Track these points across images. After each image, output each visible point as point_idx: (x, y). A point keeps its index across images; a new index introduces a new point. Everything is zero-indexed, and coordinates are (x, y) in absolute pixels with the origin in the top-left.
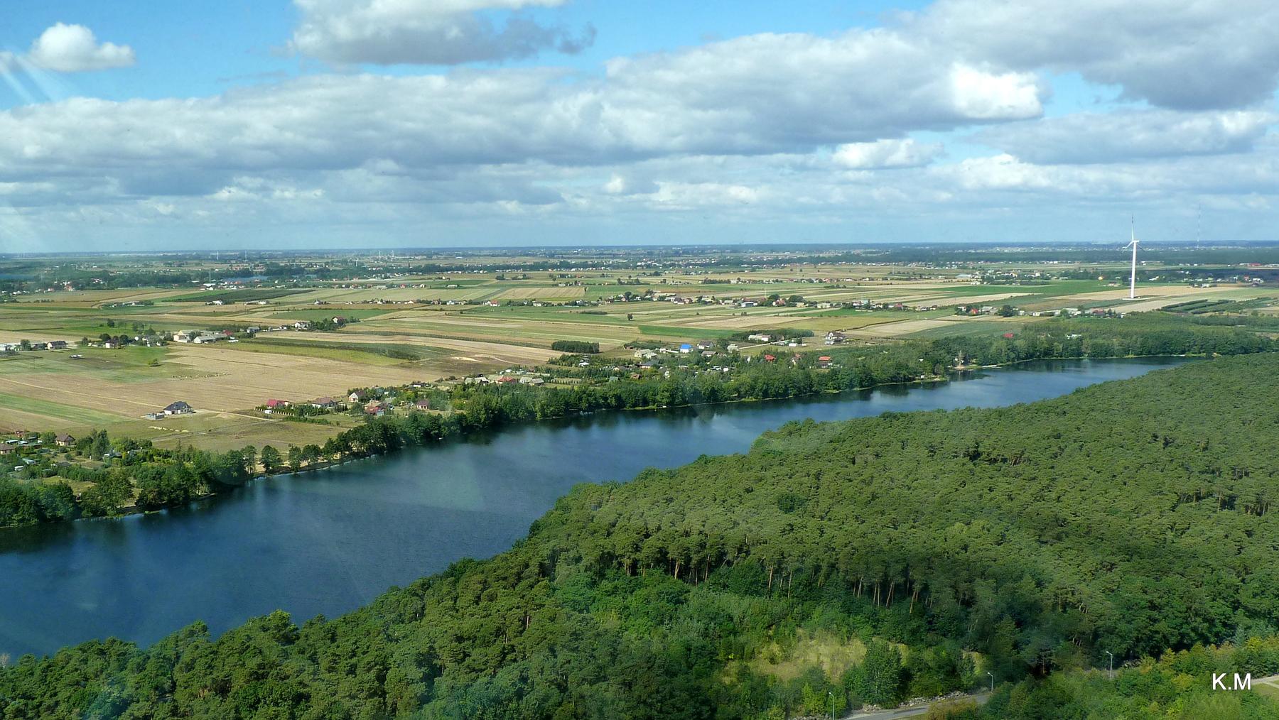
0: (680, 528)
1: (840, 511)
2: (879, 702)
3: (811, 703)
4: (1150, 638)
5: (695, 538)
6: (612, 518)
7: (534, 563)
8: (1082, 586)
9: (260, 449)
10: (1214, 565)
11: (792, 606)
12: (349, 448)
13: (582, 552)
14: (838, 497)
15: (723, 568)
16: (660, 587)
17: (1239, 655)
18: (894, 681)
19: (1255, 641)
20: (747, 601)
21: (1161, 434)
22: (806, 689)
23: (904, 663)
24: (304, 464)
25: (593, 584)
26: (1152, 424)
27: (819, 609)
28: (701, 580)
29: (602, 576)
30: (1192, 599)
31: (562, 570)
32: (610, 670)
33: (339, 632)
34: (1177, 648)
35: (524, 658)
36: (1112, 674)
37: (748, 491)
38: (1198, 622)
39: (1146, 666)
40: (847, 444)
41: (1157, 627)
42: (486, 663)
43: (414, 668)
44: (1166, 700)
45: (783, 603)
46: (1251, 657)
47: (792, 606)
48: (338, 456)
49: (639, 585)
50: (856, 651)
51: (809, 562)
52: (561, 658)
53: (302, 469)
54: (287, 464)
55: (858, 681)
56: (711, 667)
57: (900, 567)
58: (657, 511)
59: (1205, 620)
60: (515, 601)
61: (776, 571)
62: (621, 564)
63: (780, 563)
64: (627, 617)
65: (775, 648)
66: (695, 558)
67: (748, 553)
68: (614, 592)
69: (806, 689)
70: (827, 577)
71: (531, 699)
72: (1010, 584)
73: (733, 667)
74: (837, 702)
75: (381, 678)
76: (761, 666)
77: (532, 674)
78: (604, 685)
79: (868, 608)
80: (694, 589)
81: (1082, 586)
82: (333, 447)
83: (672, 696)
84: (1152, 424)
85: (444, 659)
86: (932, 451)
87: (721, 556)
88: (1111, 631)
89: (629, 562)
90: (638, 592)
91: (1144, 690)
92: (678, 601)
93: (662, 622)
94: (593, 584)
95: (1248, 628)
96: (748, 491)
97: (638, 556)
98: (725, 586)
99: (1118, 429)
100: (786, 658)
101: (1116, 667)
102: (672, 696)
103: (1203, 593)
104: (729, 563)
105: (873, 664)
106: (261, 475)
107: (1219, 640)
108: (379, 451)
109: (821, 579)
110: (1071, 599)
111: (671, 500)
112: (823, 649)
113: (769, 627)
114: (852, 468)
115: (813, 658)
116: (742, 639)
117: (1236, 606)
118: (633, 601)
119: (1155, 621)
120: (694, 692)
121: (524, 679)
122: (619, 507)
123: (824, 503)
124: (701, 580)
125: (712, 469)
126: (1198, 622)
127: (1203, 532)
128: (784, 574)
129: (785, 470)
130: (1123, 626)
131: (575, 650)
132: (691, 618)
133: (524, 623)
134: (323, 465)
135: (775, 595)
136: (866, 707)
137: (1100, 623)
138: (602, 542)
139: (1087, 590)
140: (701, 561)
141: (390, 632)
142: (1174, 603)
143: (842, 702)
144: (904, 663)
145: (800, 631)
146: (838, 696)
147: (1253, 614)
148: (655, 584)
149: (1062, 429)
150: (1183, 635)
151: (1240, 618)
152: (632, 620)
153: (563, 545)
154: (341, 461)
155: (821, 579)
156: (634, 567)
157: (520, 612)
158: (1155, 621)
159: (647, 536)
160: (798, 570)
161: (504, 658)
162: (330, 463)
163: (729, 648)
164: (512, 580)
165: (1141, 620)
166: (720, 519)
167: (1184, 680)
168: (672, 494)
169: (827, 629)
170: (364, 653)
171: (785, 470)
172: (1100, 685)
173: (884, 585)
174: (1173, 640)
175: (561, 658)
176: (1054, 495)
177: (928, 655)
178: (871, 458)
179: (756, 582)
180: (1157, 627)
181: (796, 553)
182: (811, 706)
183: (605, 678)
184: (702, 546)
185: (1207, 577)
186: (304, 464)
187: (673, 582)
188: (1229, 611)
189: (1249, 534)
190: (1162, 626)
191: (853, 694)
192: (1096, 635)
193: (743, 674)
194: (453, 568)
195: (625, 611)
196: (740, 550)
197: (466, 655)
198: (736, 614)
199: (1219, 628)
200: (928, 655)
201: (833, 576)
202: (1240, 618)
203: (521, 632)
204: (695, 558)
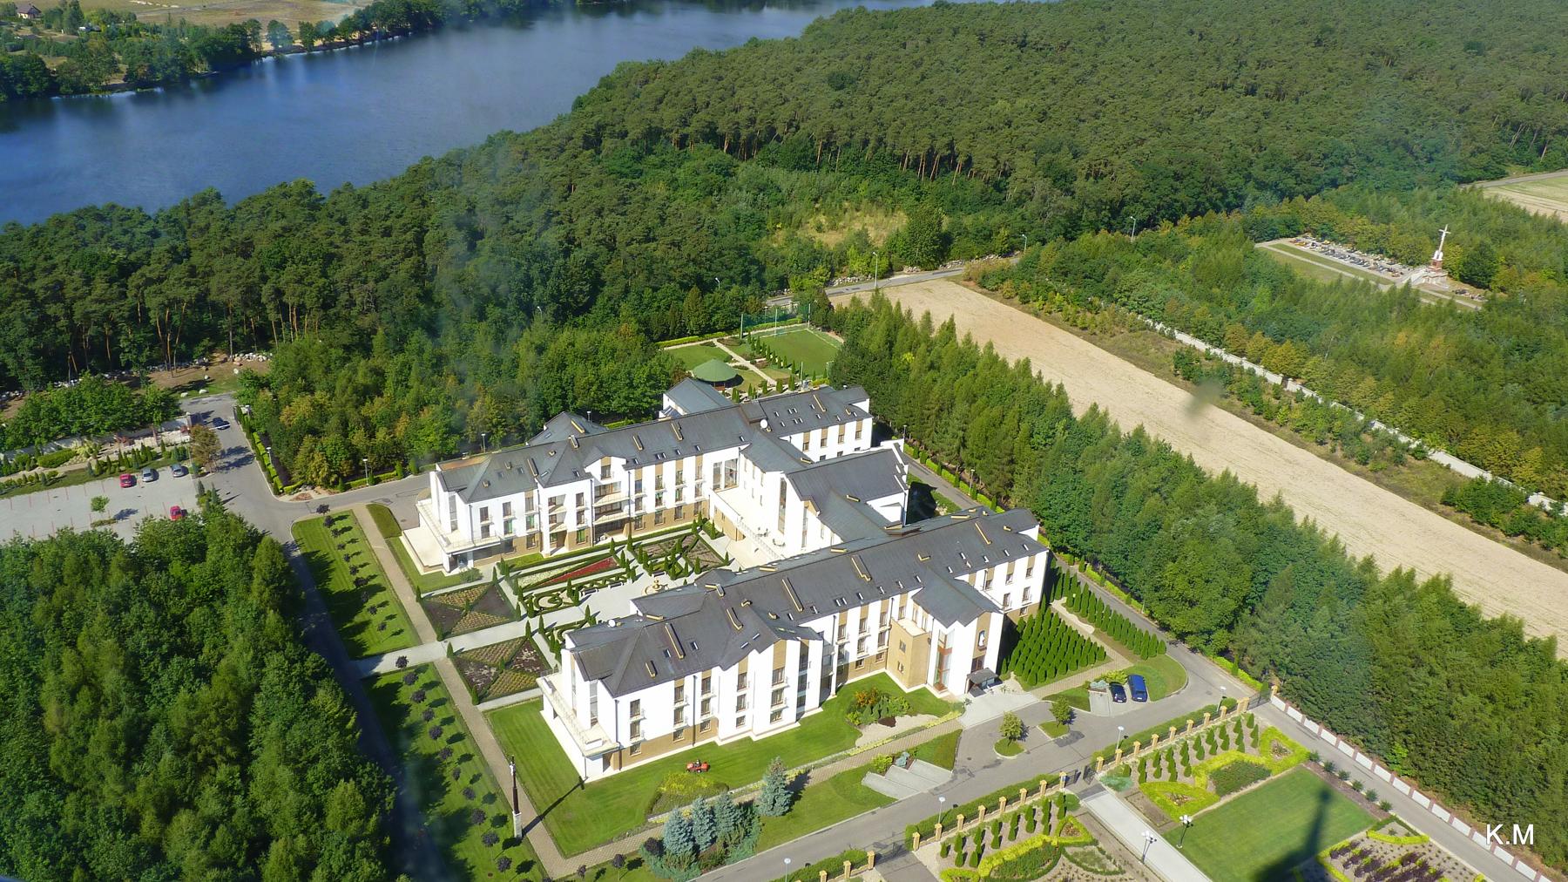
0: (730, 103)
1: (889, 90)
2: (919, 264)
3: (856, 265)
4: (1170, 206)
5: (745, 113)
6: (660, 93)
7: (578, 134)
8: (1113, 158)
9: (265, 26)
10: (1234, 140)
11: (839, 179)
12: (369, 28)
13: (628, 128)
14: (888, 78)
15: (773, 144)
16: (709, 160)
17: (1245, 221)
18: (935, 243)
19: (1260, 209)
20: (795, 175)
21: (1197, 29)
22: (851, 251)
23: (944, 228)
24: (318, 43)
25: (639, 159)
26: (1191, 20)
27: (866, 183)
28: (750, 156)
29: (650, 151)
30: (1211, 170)
31: (607, 143)
32: (659, 231)
33: (371, 199)
34: (1192, 215)
35: (571, 221)
36: (1133, 239)
37: (798, 70)
38: (1214, 194)
39: (1165, 229)
40: (899, 31)
41: (1178, 196)
42: (530, 225)
43: (454, 229)
44: (1179, 258)
45: (831, 178)
46: (1256, 223)
47: (839, 179)
48: (356, 35)
49: (688, 158)
50: (900, 222)
51: (858, 136)
52: (607, 220)
53: (317, 49)
54: (298, 43)
55: (900, 244)
56: (759, 235)
57: (946, 140)
58: (705, 87)
59: (1220, 190)
60: (559, 169)
61: (825, 146)
62: (668, 139)
63: (829, 136)
64: (675, 189)
65: (823, 219)
66: (744, 133)
67: (798, 128)
68: (663, 164)
69: (851, 251)
70: (875, 150)
71: (579, 255)
72: (1049, 156)
73: (781, 235)
74: (880, 264)
75: (419, 240)
76: (808, 232)
77: (579, 234)
78: (653, 245)
79: (912, 181)
80: (743, 164)
81: (1113, 158)
82: (349, 25)
83: (721, 255)
84: (1191, 20)
85: (484, 220)
86: (982, 38)
87: (772, 131)
88: (1136, 199)
89: (677, 136)
90: (687, 164)
91: (1162, 250)
92: (727, 173)
93: (711, 193)
94: (639, 159)
95: (1255, 199)
96: (798, 70)
97: (686, 130)
98: (774, 162)
99: (1159, 23)
100: (833, 227)
101: (1136, 234)
102: (721, 255)
103: (1221, 164)
104: (779, 139)
105: (913, 232)
106: (269, 54)
107: (1230, 208)
108: (403, 32)
109: (869, 152)
110: (1103, 170)
111: (720, 79)
112: (868, 219)
113: (816, 200)
114: (902, 52)
115: (857, 227)
116: (790, 208)
117: (1248, 177)
118: (681, 174)
119: (1176, 190)
120: (742, 251)
121: (571, 241)
122: (667, 84)
123: (875, 81)
124: (750, 156)
125: (761, 51)
126: (1214, 194)
127: (1226, 114)
128: (833, 149)
129: (836, 51)
130: (1147, 195)
131: (624, 214)
132: (740, 189)
133: (570, 188)
134: (339, 45)
135: (824, 170)
136: (907, 269)
137: (1127, 191)
138: (649, 115)
139: (1119, 162)
140: (752, 137)
141: (426, 198)
142: (1196, 174)
143: (885, 262)
144: (944, 228)
145: (846, 204)
146: (881, 257)
147: (1262, 186)
148: (703, 155)
149: (1107, 22)
150: (1199, 204)
151: (1250, 190)
152: (680, 191)
153: (608, 120)
154: (361, 41)
155: (869, 152)
156: (682, 143)
157: (566, 179)
158: (1176, 190)
159: (695, 111)
160: (848, 145)
161: (549, 221)
162: (348, 43)
163: (777, 217)
164: (554, 152)
165: (1165, 186)
166: (770, 95)
167: (1195, 242)
168: (722, 72)
169: (873, 201)
170: (399, 217)
171: (836, 51)
172: (1123, 246)
173: (930, 154)
174: (1190, 208)
175: (607, 220)
176: (1095, 79)
177: (968, 221)
178: (921, 44)
179: (805, 157)
180: (1178, 196)
181: (845, 126)
182: (855, 267)
183: (654, 239)
184: (753, 121)
185: (1226, 152)
186: (318, 43)
187: (722, 155)
188: (1241, 182)
189: (1266, 114)
190: (1182, 196)
191: (895, 256)
192: (1123, 204)
193: (790, 240)
194: (491, 141)
195: (673, 184)
196: (790, 125)
197: (508, 218)
198: (785, 187)
199: (1231, 198)
200: (968, 221)
201: (881, 150)
202: (1250, 190)
203: (565, 199)
204: (744, 133)
